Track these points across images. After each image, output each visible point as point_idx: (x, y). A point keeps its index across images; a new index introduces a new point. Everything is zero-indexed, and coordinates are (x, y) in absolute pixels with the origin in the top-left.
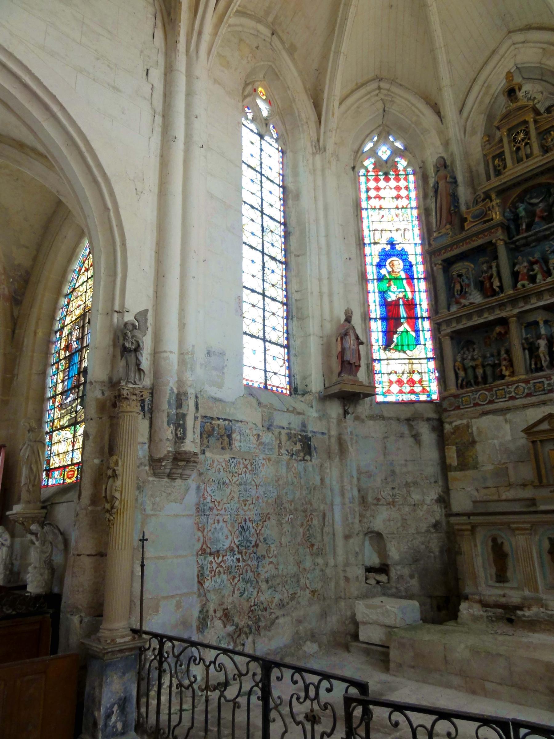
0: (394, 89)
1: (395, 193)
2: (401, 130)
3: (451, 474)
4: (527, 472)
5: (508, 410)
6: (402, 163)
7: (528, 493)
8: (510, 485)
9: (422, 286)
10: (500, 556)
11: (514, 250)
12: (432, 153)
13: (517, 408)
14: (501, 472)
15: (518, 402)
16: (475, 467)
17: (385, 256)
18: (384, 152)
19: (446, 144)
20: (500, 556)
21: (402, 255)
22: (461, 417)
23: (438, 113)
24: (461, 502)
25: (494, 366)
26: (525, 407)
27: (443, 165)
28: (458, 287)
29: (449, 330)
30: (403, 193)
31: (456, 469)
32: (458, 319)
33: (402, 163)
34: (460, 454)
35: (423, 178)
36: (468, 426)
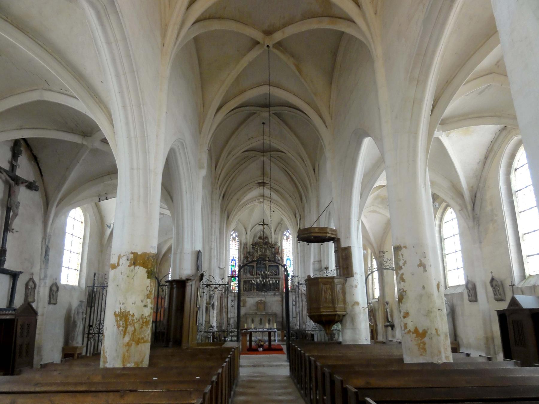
4: (255, 308)
6: (237, 238)
9: (237, 268)
11: (257, 268)
12: (244, 241)
17: (232, 260)
18: (234, 235)
19: (246, 238)
21: (235, 260)
23: (246, 231)
24: (243, 312)
27: (246, 244)
33: (237, 238)
35: (240, 244)
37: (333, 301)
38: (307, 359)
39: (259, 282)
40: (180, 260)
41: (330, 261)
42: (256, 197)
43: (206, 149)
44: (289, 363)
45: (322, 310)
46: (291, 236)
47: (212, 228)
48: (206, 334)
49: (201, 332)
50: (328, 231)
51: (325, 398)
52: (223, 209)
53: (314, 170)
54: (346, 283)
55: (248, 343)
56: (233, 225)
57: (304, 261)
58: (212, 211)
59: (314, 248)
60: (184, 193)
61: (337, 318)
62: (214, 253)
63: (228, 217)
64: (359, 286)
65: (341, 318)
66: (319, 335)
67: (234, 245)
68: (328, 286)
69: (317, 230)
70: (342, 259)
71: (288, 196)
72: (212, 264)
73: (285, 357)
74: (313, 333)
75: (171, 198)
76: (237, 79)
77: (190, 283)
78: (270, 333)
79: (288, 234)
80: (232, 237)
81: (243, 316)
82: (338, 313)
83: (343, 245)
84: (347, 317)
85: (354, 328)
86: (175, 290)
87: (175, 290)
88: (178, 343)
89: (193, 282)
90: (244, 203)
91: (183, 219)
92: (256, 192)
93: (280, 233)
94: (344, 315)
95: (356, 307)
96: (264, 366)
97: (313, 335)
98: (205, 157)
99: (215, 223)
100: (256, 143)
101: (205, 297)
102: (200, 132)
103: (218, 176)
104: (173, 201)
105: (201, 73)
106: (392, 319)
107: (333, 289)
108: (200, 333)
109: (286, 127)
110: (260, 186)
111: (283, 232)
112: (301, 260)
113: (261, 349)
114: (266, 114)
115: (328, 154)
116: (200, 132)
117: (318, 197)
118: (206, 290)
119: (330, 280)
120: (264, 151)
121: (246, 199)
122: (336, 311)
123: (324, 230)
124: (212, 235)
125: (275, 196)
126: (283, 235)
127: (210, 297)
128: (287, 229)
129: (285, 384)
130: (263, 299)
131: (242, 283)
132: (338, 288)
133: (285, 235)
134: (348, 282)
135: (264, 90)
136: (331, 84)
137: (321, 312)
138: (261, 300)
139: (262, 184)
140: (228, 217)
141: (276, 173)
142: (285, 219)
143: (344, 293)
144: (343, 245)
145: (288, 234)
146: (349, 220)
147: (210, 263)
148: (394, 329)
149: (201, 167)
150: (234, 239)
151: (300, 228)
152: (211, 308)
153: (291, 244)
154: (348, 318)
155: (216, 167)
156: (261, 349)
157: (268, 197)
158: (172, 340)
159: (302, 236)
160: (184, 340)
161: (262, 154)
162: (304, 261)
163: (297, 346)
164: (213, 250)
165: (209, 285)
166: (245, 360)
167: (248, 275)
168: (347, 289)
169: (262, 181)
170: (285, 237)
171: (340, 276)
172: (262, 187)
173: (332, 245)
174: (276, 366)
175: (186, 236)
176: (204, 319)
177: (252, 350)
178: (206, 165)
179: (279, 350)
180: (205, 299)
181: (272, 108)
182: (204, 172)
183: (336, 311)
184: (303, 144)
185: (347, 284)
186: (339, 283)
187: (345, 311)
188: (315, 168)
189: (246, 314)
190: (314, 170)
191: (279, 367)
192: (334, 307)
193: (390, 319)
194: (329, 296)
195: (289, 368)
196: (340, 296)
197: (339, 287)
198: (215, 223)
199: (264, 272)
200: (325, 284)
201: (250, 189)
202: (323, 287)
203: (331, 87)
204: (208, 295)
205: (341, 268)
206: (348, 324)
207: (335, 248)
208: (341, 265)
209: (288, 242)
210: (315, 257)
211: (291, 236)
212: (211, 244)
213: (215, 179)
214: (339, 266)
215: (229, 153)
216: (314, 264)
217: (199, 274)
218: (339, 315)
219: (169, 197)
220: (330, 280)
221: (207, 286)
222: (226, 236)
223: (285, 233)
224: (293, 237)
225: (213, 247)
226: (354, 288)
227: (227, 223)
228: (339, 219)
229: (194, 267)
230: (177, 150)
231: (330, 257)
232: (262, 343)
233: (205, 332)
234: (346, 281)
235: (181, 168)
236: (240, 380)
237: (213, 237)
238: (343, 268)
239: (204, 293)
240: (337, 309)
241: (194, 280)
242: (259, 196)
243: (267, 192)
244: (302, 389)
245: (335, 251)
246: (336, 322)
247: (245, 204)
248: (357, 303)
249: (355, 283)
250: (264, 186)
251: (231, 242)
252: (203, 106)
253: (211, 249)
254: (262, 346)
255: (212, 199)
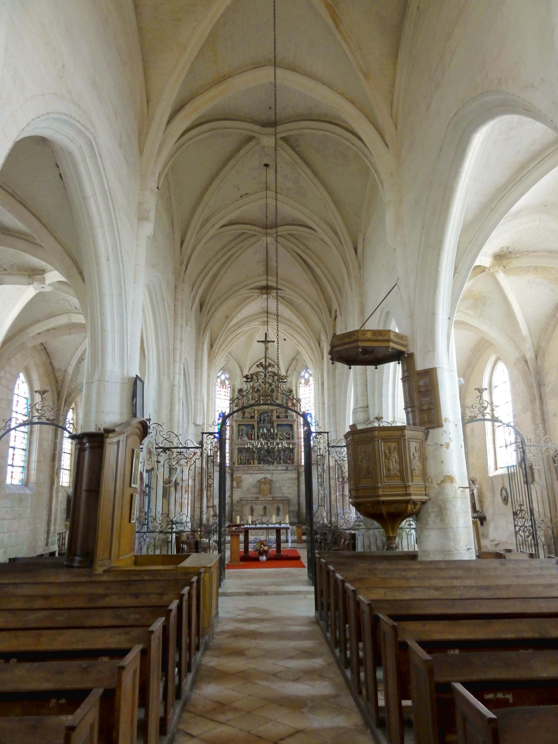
0: (231, 358)
1: (224, 393)
2: (230, 372)
3: (234, 489)
4: (255, 490)
5: (252, 474)
6: (227, 382)
7: (254, 496)
8: (250, 493)
10: (252, 510)
13: (255, 473)
14: (248, 490)
15: (255, 472)
16: (241, 488)
18: (223, 377)
20: (252, 510)
22: (239, 474)
25: (248, 460)
26: (257, 473)
28: (241, 433)
29: (238, 447)
30: (227, 394)
31: (236, 488)
32: (241, 445)
34: (237, 484)
35: (233, 391)
36: (241, 477)
37: (403, 474)
38: (366, 609)
39: (259, 446)
40: (99, 394)
41: (384, 406)
42: (256, 314)
43: (152, 183)
44: (312, 588)
45: (380, 492)
46: (311, 379)
47: (174, 349)
48: (162, 536)
49: (153, 532)
50: (392, 337)
51: (406, 703)
52: (200, 331)
53: (356, 249)
54: (426, 439)
55: (242, 546)
56: (220, 361)
57: (335, 414)
58: (175, 320)
59: (356, 386)
60: (103, 261)
61: (410, 507)
62: (180, 393)
63: (212, 347)
64: (453, 446)
65: (418, 507)
66: (369, 537)
67: (223, 393)
68: (393, 445)
69: (369, 335)
70: (419, 392)
71: (308, 310)
72: (176, 413)
73: (303, 573)
74: (353, 532)
75: (81, 273)
76: (211, 42)
77: (115, 440)
78: (278, 531)
79: (307, 376)
80: (219, 380)
81: (238, 502)
82: (413, 497)
83: (420, 366)
84: (429, 504)
85: (445, 528)
86: (87, 453)
87: (87, 453)
88: (89, 558)
89: (122, 438)
90: (237, 324)
91: (102, 314)
92: (256, 305)
93: (295, 373)
94: (423, 503)
95: (448, 485)
96: (266, 594)
97: (353, 537)
98: (151, 201)
99: (181, 341)
100: (253, 208)
101: (161, 469)
102: (141, 152)
103: (186, 258)
104: (83, 280)
105: (140, 29)
106: (482, 507)
107: (401, 451)
108: (152, 535)
109: (307, 170)
110: (262, 294)
111: (300, 373)
112: (329, 413)
113: (264, 558)
114: (268, 141)
115: (387, 195)
116: (141, 152)
117: (362, 295)
118: (163, 457)
119: (398, 433)
120: (270, 225)
121: (240, 316)
122: (410, 495)
123: (383, 335)
124: (174, 361)
125: (285, 312)
126: (299, 376)
127: (171, 470)
128: (307, 368)
129: (307, 644)
130: (269, 476)
131: (236, 452)
132: (413, 450)
133: (304, 376)
134: (429, 437)
135: (265, 75)
136: (396, 55)
137: (379, 496)
138: (265, 478)
139: (266, 289)
140: (212, 347)
141: (289, 269)
142: (303, 351)
143: (424, 459)
144: (420, 366)
145: (307, 376)
146: (433, 314)
147: (171, 411)
148: (484, 523)
149: (142, 218)
150: (223, 383)
151: (334, 334)
152: (173, 489)
153: (313, 391)
154: (430, 508)
155: (182, 243)
156: (264, 558)
157: (274, 314)
158: (79, 552)
159: (338, 349)
160: (101, 553)
161: (265, 231)
162: (335, 414)
163: (326, 555)
164: (176, 389)
165: (168, 449)
166: (236, 580)
167: (245, 438)
168: (430, 450)
169: (264, 283)
170: (303, 381)
171: (414, 424)
172: (265, 296)
173: (393, 371)
174: (289, 593)
175: (109, 348)
176: (159, 509)
177: (248, 559)
178: (152, 215)
179: (292, 559)
180: (162, 473)
181: (280, 128)
182: (148, 228)
183: (410, 495)
184: (336, 202)
185: (429, 441)
186: (413, 438)
187: (426, 495)
188: (357, 247)
189: (241, 500)
190: (356, 249)
191: (293, 598)
192: (406, 487)
193: (478, 508)
194: (394, 466)
195: (313, 596)
196: (417, 464)
197: (413, 446)
198: (181, 341)
199: (269, 431)
200: (385, 440)
201: (246, 300)
202: (382, 446)
203: (395, 64)
204: (167, 466)
205: (417, 413)
206: (432, 519)
207: (403, 372)
208: (416, 403)
209: (307, 388)
210: (356, 401)
211: (311, 379)
212: (174, 378)
213: (181, 265)
214: (413, 407)
215: (207, 220)
216: (355, 412)
217: (135, 421)
218: (414, 503)
219: (75, 272)
220: (398, 433)
221: (165, 449)
222: (209, 376)
223: (303, 374)
224: (315, 380)
225: (176, 383)
226: (444, 449)
227: (209, 356)
228: (412, 316)
229: (127, 410)
230: (79, 158)
231: (383, 399)
232: (266, 548)
233: (161, 532)
234: (427, 434)
235: (91, 201)
236: (218, 629)
237: (177, 365)
238: (422, 411)
239: (158, 462)
240: (411, 490)
241: (122, 433)
242: (261, 313)
243: (272, 305)
244: (348, 663)
245: (404, 379)
246: (409, 516)
247: (239, 325)
248: (450, 479)
249: (444, 440)
250: (267, 294)
251: (218, 389)
252: (148, 102)
253: (173, 386)
254: (265, 552)
255: (176, 299)
